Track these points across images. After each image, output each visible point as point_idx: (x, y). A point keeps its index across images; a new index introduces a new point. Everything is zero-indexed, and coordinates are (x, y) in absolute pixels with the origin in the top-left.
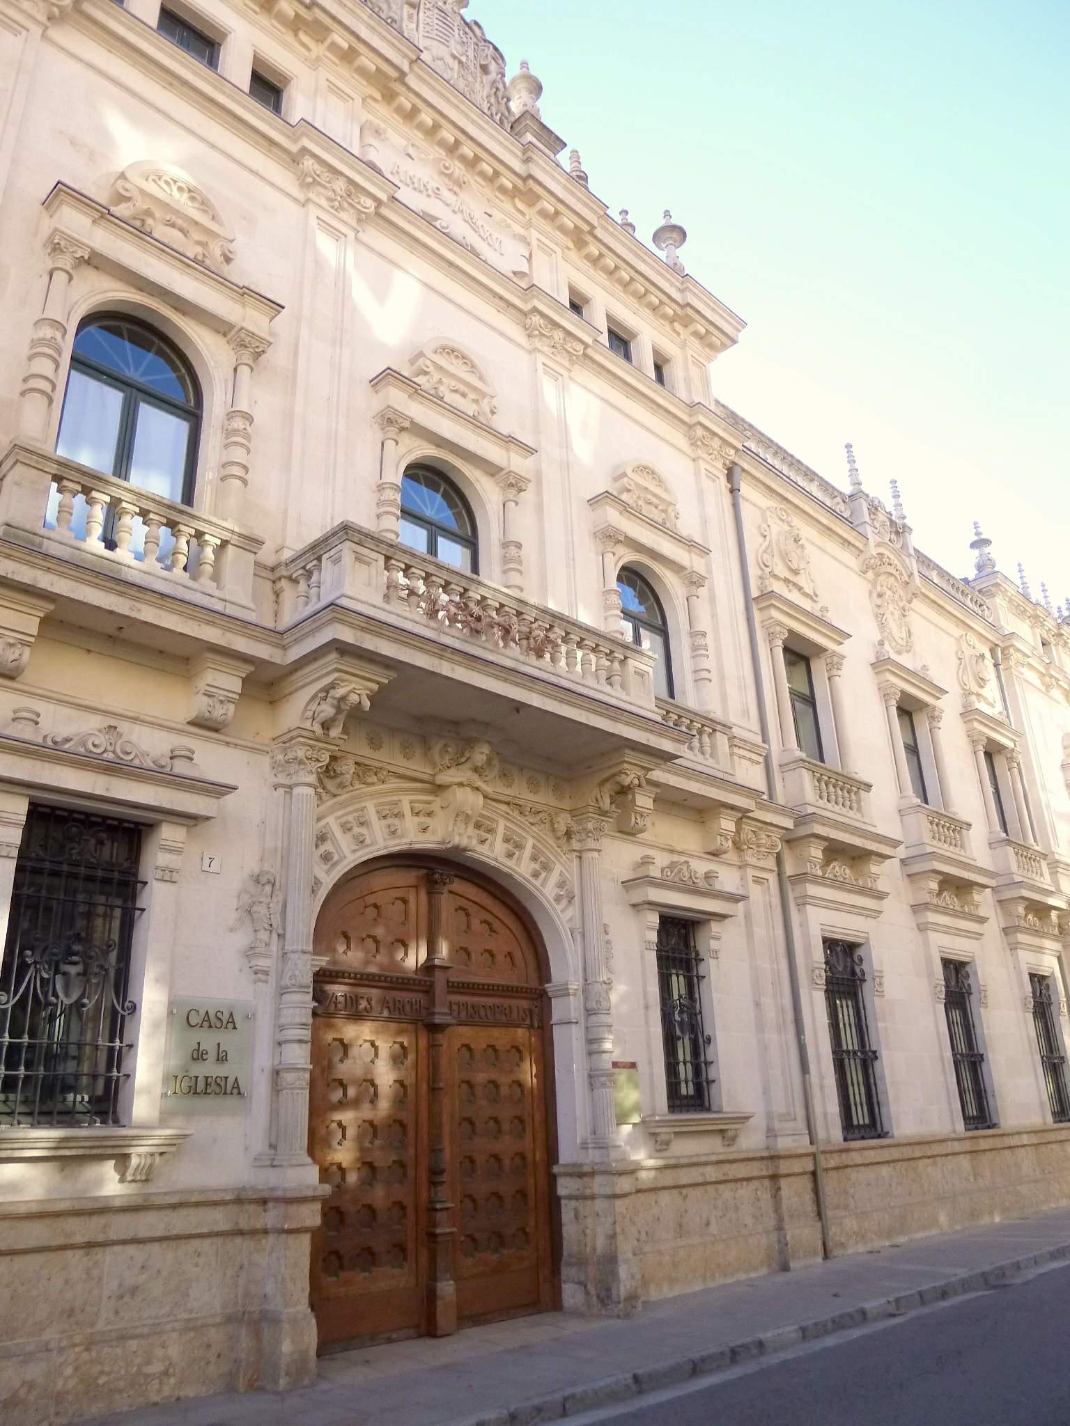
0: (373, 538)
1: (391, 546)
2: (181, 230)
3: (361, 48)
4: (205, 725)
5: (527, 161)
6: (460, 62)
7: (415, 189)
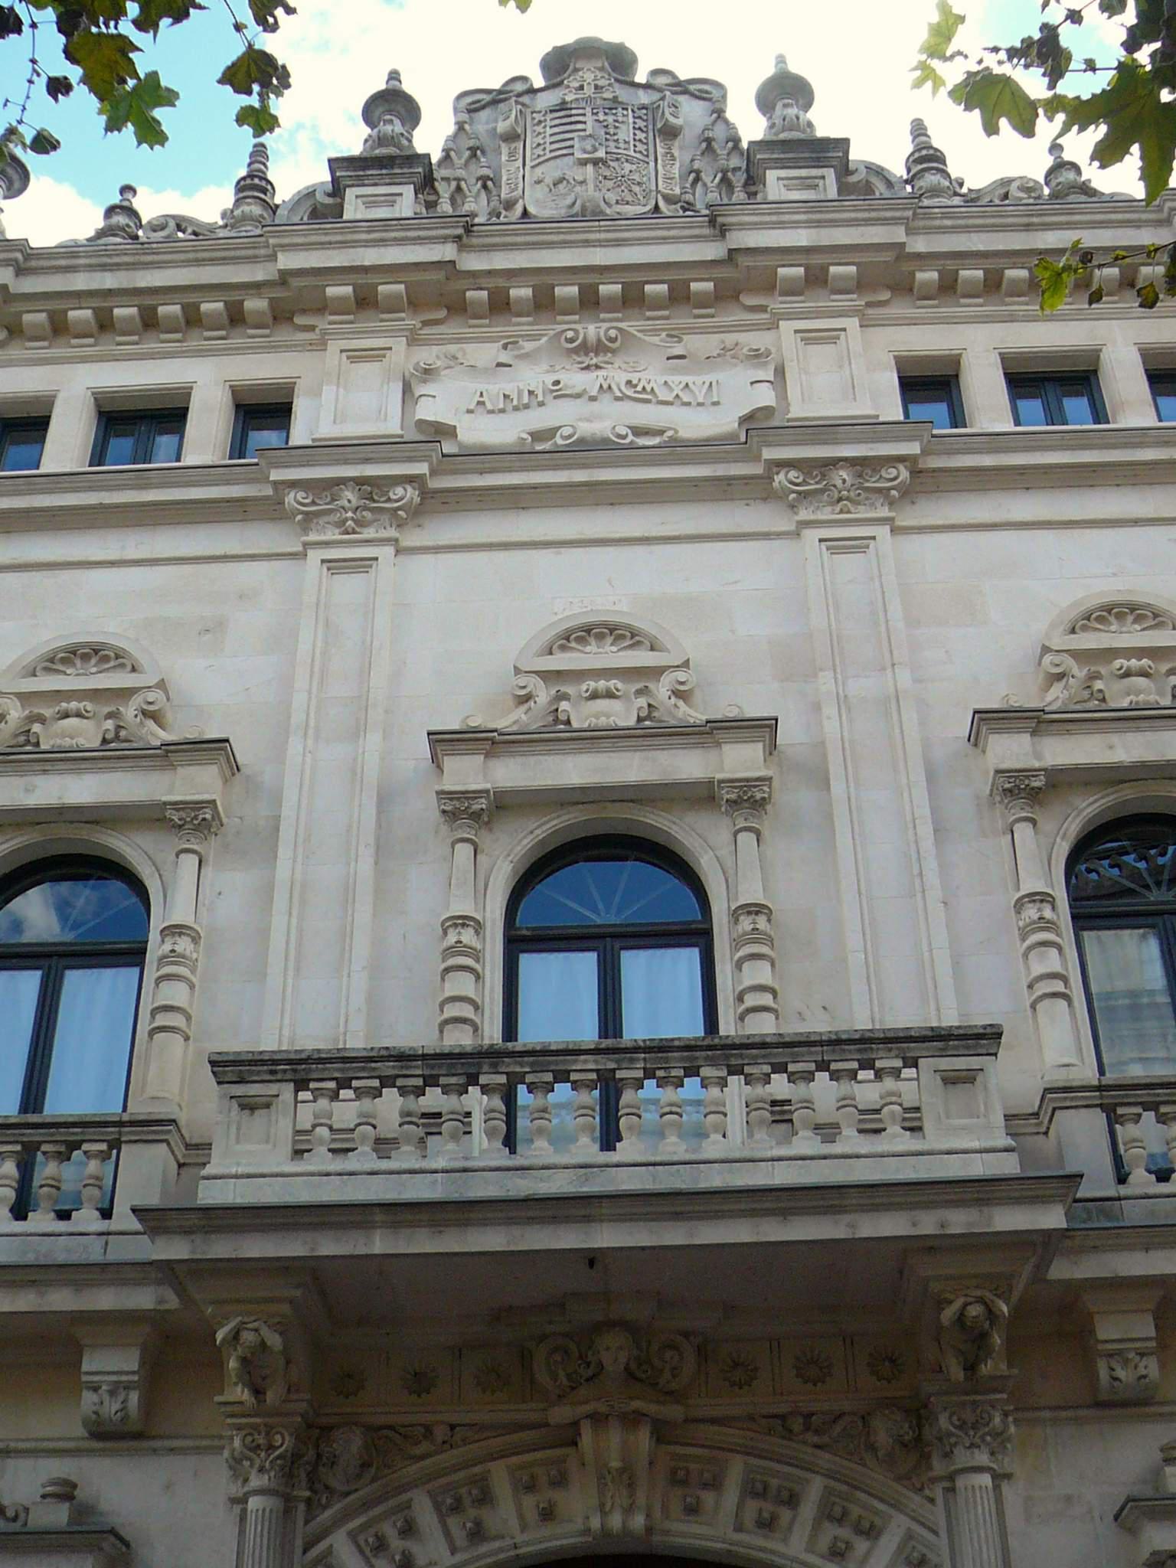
0: (263, 1062)
1: (301, 1062)
2: (79, 715)
3: (371, 279)
4: (107, 1436)
5: (722, 231)
6: (596, 162)
7: (516, 409)
